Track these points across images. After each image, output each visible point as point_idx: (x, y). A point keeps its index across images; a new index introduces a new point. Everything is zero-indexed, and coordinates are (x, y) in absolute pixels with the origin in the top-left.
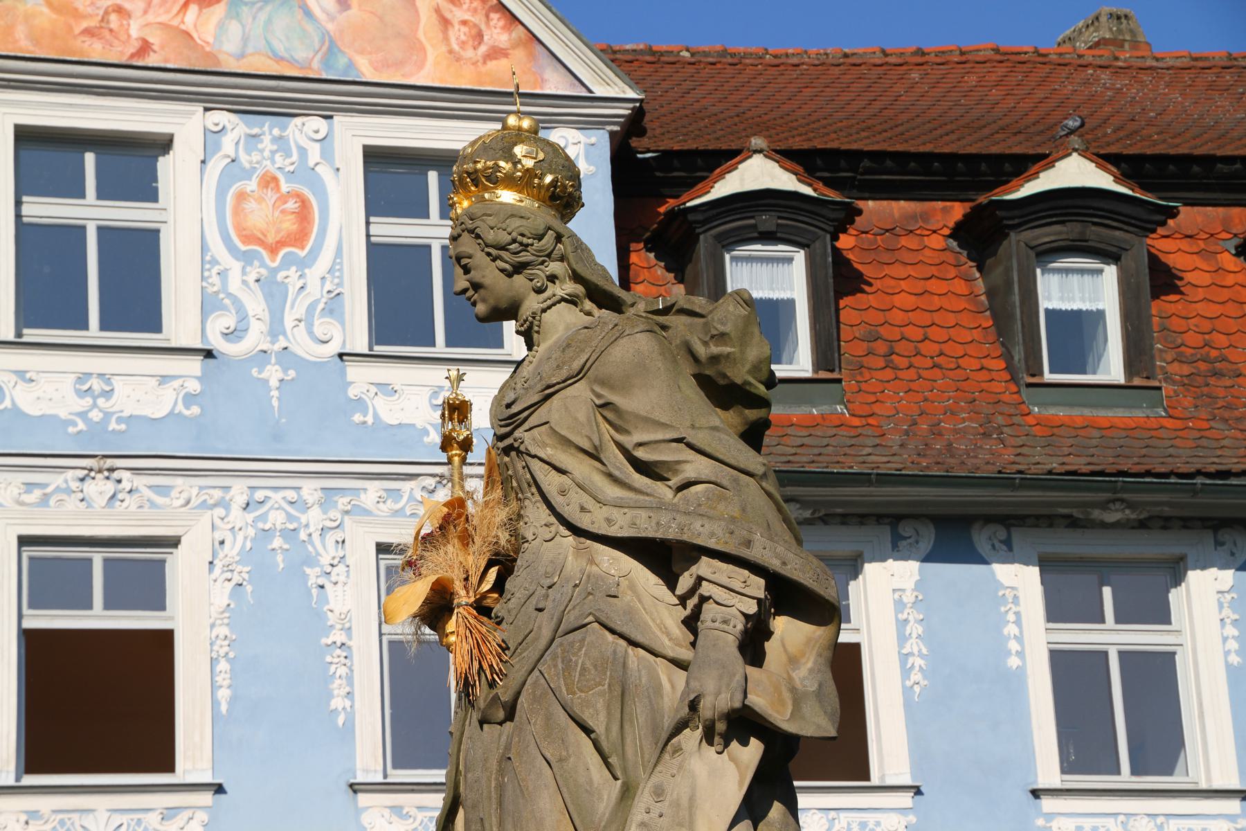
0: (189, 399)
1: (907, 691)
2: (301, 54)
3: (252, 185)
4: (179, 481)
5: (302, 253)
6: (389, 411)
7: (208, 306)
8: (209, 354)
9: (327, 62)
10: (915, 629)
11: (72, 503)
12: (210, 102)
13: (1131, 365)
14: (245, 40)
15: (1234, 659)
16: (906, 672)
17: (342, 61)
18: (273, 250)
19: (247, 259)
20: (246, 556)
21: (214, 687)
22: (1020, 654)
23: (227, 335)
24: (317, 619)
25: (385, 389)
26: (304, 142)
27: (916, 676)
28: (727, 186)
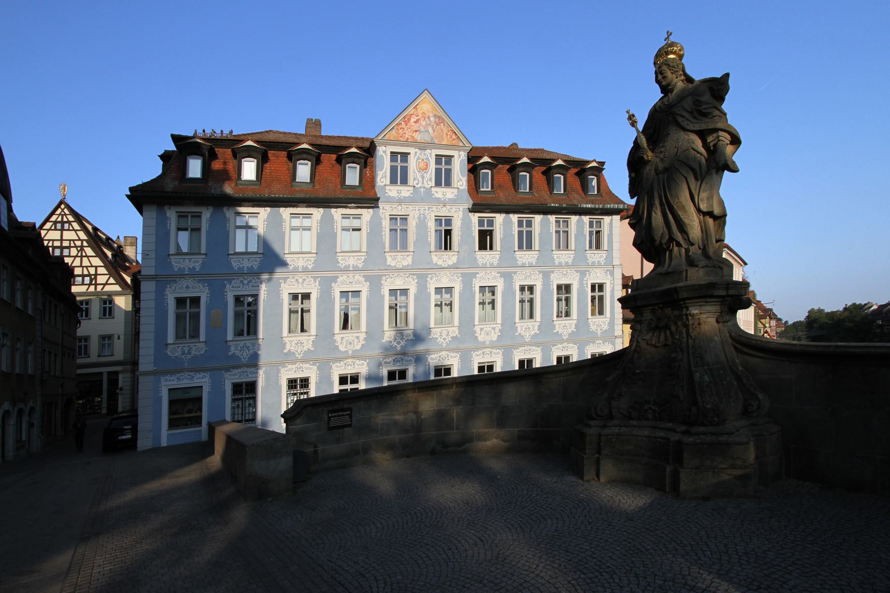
0: (411, 194)
2: (428, 140)
3: (420, 161)
4: (410, 206)
6: (437, 196)
7: (414, 179)
8: (414, 186)
10: (502, 228)
11: (396, 210)
12: (416, 147)
14: (421, 137)
17: (433, 141)
19: (419, 172)
20: (418, 218)
23: (417, 184)
25: (437, 192)
27: (502, 235)
28: (481, 161)
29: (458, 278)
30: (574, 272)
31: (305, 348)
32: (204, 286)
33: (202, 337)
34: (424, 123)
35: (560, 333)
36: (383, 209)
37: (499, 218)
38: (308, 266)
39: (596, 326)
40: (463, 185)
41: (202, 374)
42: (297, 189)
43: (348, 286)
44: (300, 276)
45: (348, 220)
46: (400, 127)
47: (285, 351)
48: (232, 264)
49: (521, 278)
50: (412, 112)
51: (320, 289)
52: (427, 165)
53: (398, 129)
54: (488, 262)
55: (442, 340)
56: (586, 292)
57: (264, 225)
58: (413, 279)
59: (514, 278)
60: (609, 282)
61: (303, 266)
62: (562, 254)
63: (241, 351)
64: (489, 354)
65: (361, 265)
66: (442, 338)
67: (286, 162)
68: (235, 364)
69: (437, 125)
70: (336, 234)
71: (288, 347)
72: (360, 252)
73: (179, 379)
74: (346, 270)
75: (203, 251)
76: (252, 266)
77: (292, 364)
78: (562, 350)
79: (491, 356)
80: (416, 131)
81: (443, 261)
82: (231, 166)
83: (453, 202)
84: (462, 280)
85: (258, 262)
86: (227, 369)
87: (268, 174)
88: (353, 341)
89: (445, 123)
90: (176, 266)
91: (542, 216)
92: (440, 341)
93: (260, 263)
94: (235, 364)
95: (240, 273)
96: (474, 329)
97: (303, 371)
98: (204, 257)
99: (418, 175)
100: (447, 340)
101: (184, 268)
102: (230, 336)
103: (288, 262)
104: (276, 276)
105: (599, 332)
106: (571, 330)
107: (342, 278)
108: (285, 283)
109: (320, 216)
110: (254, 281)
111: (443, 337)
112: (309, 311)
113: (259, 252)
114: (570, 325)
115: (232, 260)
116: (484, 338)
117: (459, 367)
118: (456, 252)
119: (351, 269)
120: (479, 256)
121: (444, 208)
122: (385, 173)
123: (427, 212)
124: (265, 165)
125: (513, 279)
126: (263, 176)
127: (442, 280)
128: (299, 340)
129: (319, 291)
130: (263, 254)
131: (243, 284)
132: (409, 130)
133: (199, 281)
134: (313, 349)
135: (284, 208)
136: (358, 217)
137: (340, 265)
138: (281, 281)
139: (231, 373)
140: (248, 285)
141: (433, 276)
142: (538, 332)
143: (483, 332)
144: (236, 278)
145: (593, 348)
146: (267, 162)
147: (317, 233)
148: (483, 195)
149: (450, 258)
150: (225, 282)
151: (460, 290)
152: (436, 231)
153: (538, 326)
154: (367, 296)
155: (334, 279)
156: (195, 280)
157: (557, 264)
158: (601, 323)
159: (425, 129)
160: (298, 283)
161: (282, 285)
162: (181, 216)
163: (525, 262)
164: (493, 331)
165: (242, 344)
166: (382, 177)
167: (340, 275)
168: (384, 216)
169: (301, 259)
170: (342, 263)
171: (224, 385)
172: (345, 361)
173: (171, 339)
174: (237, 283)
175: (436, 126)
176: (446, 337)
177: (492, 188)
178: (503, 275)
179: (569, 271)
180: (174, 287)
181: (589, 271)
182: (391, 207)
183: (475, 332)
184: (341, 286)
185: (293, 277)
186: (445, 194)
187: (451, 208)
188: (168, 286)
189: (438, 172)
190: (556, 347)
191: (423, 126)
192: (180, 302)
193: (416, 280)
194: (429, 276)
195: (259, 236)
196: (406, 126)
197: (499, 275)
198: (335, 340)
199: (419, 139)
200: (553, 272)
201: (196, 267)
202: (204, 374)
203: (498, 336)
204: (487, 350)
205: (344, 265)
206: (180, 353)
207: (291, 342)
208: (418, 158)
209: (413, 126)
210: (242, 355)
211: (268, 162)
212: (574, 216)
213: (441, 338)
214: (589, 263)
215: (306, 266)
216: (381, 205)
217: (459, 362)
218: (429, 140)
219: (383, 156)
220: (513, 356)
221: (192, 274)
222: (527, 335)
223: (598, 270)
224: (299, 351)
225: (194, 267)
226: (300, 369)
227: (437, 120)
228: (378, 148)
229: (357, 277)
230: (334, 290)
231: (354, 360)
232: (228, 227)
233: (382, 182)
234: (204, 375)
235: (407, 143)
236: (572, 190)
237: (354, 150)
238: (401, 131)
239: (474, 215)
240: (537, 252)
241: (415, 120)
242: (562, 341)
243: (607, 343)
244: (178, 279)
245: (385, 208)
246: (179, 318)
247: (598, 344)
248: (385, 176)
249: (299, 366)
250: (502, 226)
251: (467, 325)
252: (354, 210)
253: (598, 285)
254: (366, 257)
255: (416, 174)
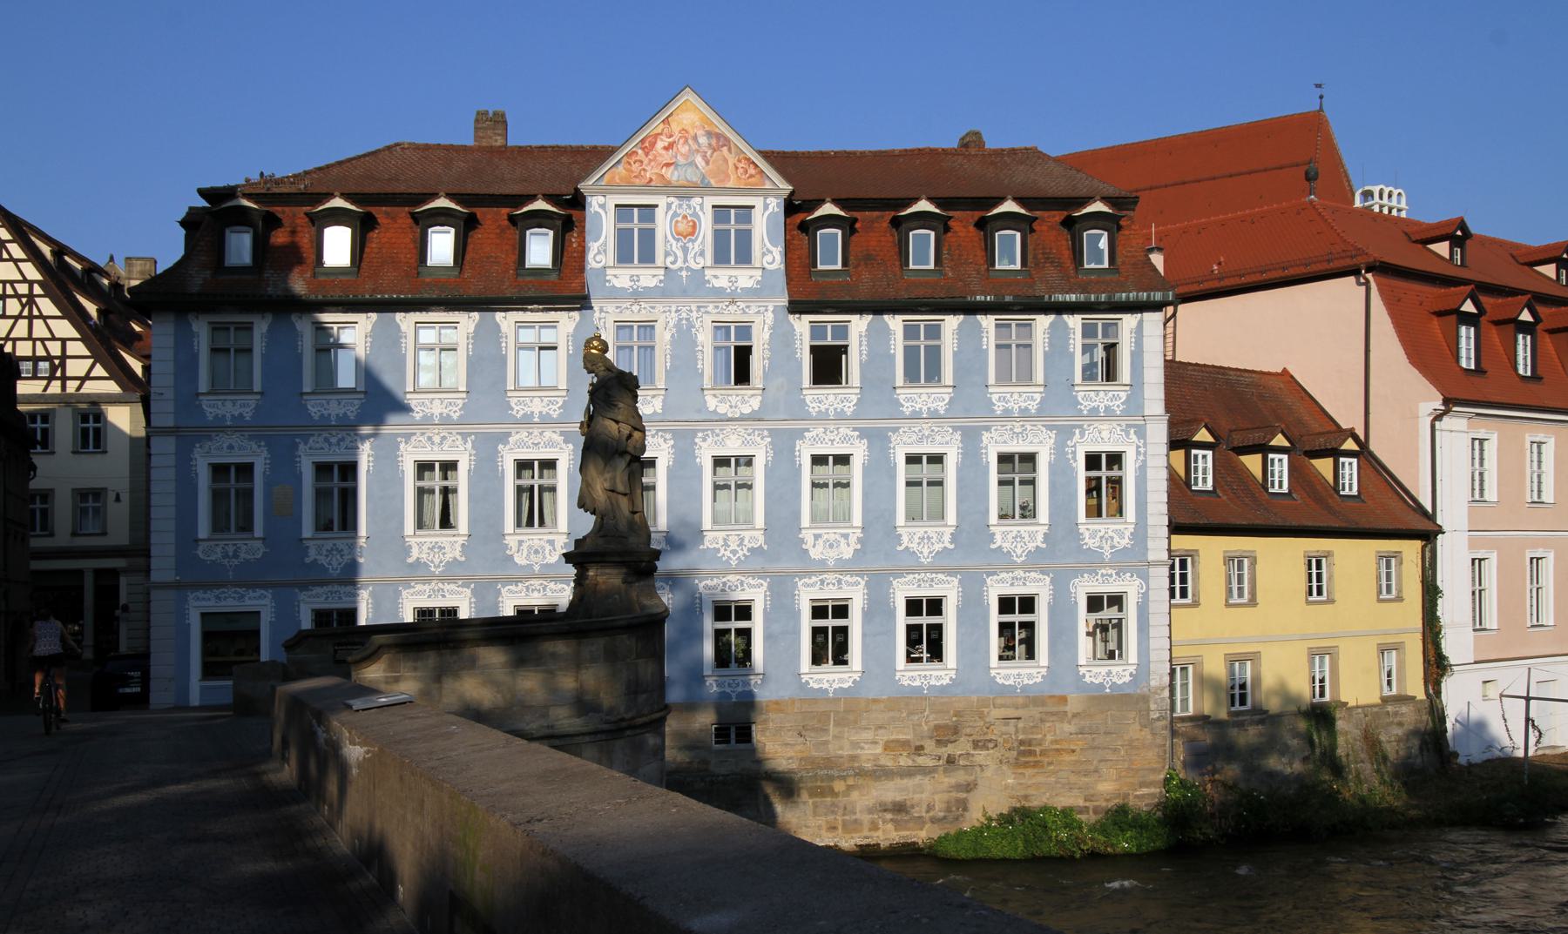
0: (661, 281)
1: (861, 361)
2: (694, 180)
3: (680, 219)
4: (658, 305)
5: (693, 238)
6: (717, 283)
7: (667, 254)
9: (702, 181)
11: (628, 312)
13: (936, 265)
14: (679, 177)
15: (955, 349)
16: (861, 355)
18: (685, 238)
19: (678, 240)
20: (675, 326)
21: (666, 362)
22: (894, 349)
23: (672, 263)
24: (695, 343)
26: (695, 205)
27: (864, 356)
28: (818, 213)
29: (762, 439)
30: (1044, 429)
31: (449, 557)
32: (259, 446)
33: (259, 530)
34: (684, 149)
35: (1005, 550)
36: (601, 310)
37: (858, 325)
38: (452, 414)
39: (1098, 538)
40: (774, 260)
41: (260, 592)
42: (428, 280)
43: (531, 450)
44: (437, 431)
45: (533, 330)
46: (634, 158)
47: (410, 560)
48: (308, 409)
49: (909, 441)
50: (659, 130)
51: (475, 455)
52: (694, 226)
53: (630, 164)
54: (832, 409)
55: (728, 553)
56: (1074, 471)
57: (366, 342)
58: (665, 440)
59: (893, 439)
60: (1134, 448)
61: (441, 414)
62: (1013, 393)
63: (327, 556)
64: (834, 584)
65: (557, 413)
66: (729, 549)
67: (411, 228)
68: (317, 578)
69: (715, 150)
70: (504, 359)
71: (415, 553)
72: (555, 389)
73: (218, 598)
74: (527, 421)
75: (257, 387)
76: (345, 413)
77: (424, 584)
78: (1012, 584)
79: (841, 588)
80: (668, 165)
81: (731, 407)
82: (305, 240)
83: (751, 293)
84: (770, 443)
85: (357, 407)
86: (305, 586)
87: (376, 250)
88: (543, 548)
89: (732, 146)
90: (211, 413)
91: (961, 317)
92: (724, 555)
93: (359, 408)
94: (317, 578)
95: (324, 425)
96: (800, 536)
97: (444, 596)
98: (258, 397)
99: (676, 247)
100: (741, 553)
101: (224, 416)
102: (308, 530)
103: (413, 407)
104: (386, 430)
105: (1107, 554)
106: (1034, 545)
107: (518, 437)
108: (406, 443)
109: (474, 325)
110: (350, 439)
111: (731, 548)
112: (455, 491)
113: (358, 390)
114: (1032, 536)
115: (308, 402)
116: (822, 553)
117: (765, 605)
118: (758, 389)
119: (536, 420)
120: (811, 397)
121: (732, 308)
122: (605, 244)
123: (694, 314)
124: (371, 234)
125: (891, 442)
126: (365, 256)
127: (728, 442)
128: (436, 543)
129: (473, 458)
130: (365, 393)
131: (330, 444)
132: (653, 163)
133: (251, 438)
134: (463, 559)
135: (403, 314)
136: (552, 325)
137: (514, 413)
138: (399, 439)
139: (310, 593)
140: (339, 445)
141: (707, 435)
142: (952, 547)
143: (820, 541)
144: (316, 433)
145: (1091, 583)
146: (373, 229)
147: (468, 355)
148: (821, 280)
149: (747, 400)
150: (297, 440)
151: (767, 461)
152: (717, 348)
153: (952, 534)
154: (569, 469)
155: (504, 438)
156: (242, 435)
157: (999, 412)
158: (1110, 534)
159: (687, 159)
160: (433, 443)
161: (402, 446)
162: (216, 328)
163: (921, 409)
164: (843, 541)
165: (329, 544)
166: (599, 253)
167: (513, 431)
168: (602, 324)
169: (437, 402)
170: (518, 410)
171: (299, 612)
172: (527, 584)
173: (204, 530)
174: (318, 442)
175: (713, 153)
176: (738, 549)
177: (845, 263)
178: (864, 434)
179: (1029, 428)
180: (207, 446)
181: (1081, 427)
182: (617, 307)
183: (802, 541)
184: (516, 451)
185: (423, 434)
186: (733, 279)
187: (748, 307)
188: (198, 445)
189: (720, 238)
190: (995, 577)
191: (682, 154)
192: (219, 471)
193: (672, 442)
194: (700, 435)
195: (357, 361)
196: (647, 156)
197: (858, 433)
198: (507, 545)
199: (675, 178)
200: (988, 429)
201: (245, 415)
202: (263, 591)
203: (855, 550)
204: (830, 577)
205: (521, 413)
206: (220, 555)
207: (420, 545)
208: (675, 215)
209: (660, 155)
210: (330, 564)
211: (376, 228)
212: (1043, 316)
213: (725, 550)
214: (1081, 410)
215: (448, 415)
216: (595, 304)
217: (766, 596)
218: (696, 179)
219: (599, 213)
220: (892, 591)
221: (239, 426)
222: (926, 552)
223: (1105, 427)
224: (437, 561)
225: (241, 415)
226: (438, 591)
227: (714, 142)
228: (589, 199)
229: (548, 434)
230: (502, 457)
231: (545, 583)
232: (300, 348)
233: (599, 262)
234: (262, 594)
235: (648, 187)
236: (1048, 258)
237: (540, 205)
238: (635, 167)
239: (799, 318)
240: (950, 390)
241: (666, 144)
242: (1010, 566)
243: (1129, 574)
244: (213, 434)
245: (604, 309)
246: (218, 497)
247: (1103, 575)
248: (605, 251)
249: (436, 588)
250: (863, 339)
251: (783, 526)
252: (541, 313)
253: (1107, 455)
254: (566, 398)
255: (671, 245)
